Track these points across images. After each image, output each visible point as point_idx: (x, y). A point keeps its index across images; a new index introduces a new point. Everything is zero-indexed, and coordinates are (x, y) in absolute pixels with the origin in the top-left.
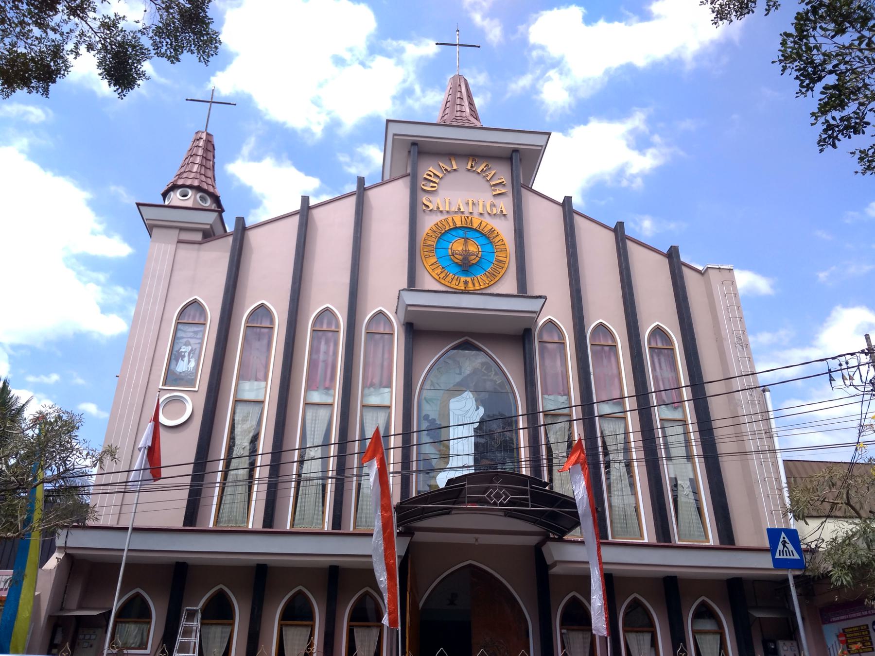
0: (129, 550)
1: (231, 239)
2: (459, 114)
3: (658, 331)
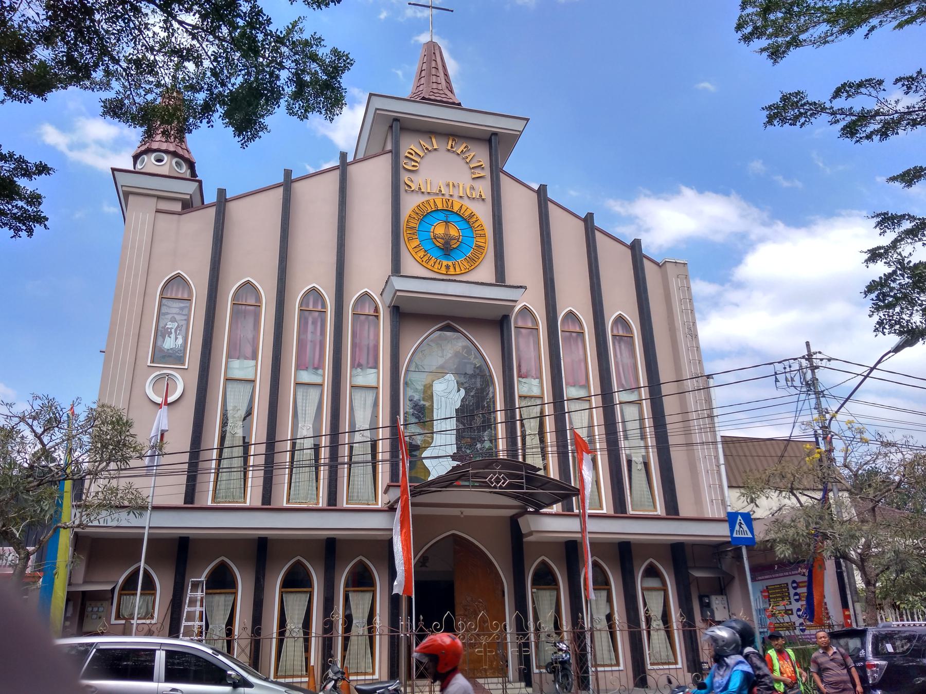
0: (150, 528)
1: (213, 211)
2: (435, 86)
3: (620, 320)
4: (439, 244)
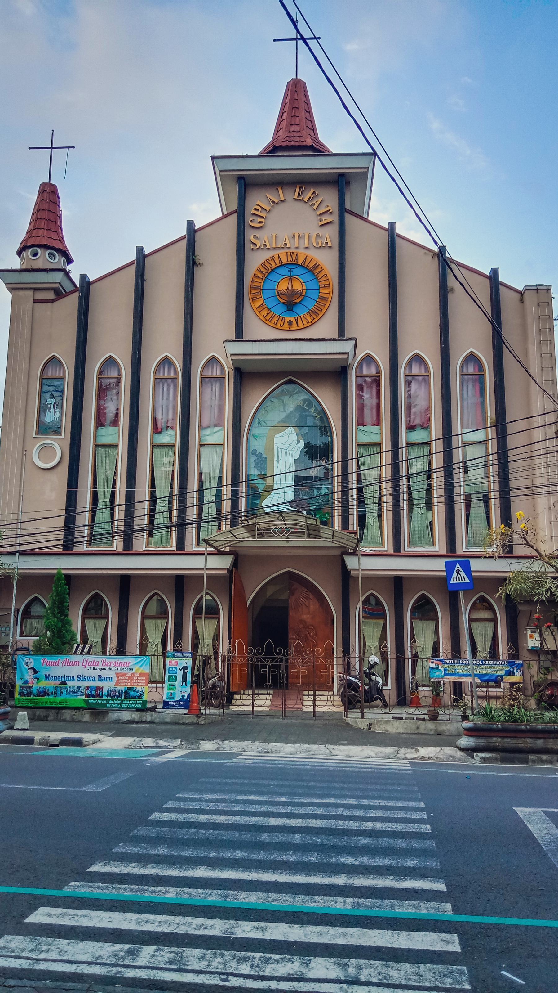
4: (282, 301)
